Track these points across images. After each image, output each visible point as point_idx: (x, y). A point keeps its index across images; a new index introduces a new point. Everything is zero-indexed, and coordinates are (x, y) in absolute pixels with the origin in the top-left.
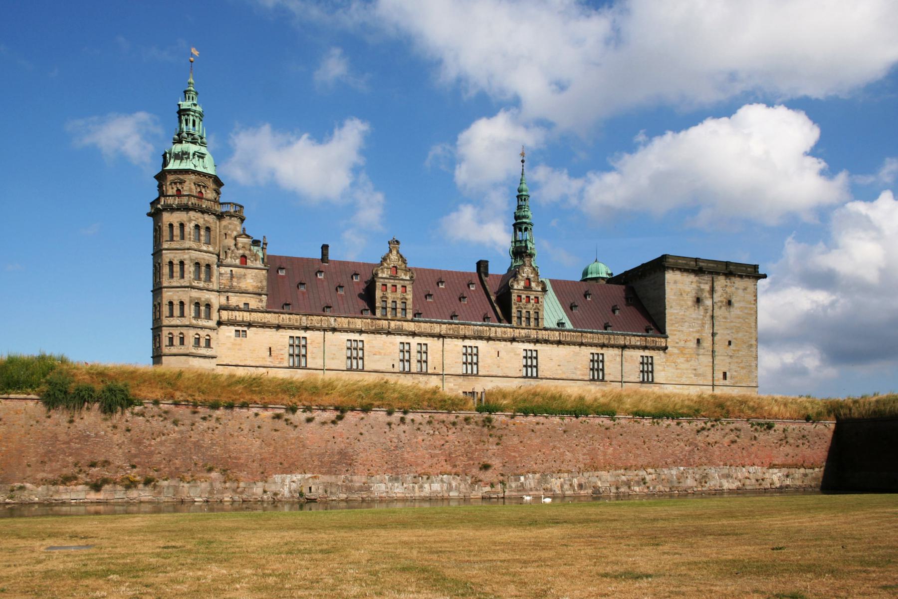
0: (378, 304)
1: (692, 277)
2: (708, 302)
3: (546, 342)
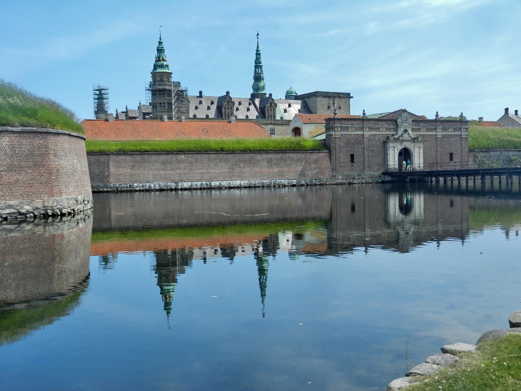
0: (223, 114)
1: (327, 99)
2: (332, 108)
3: (277, 124)
